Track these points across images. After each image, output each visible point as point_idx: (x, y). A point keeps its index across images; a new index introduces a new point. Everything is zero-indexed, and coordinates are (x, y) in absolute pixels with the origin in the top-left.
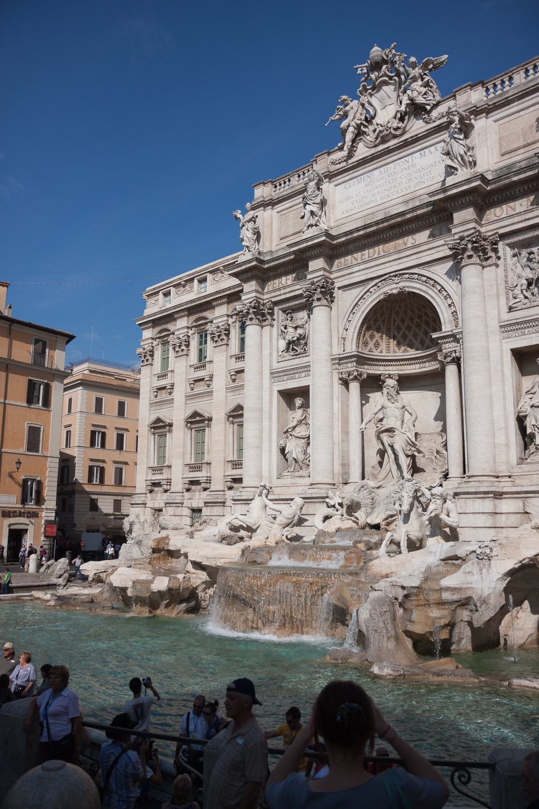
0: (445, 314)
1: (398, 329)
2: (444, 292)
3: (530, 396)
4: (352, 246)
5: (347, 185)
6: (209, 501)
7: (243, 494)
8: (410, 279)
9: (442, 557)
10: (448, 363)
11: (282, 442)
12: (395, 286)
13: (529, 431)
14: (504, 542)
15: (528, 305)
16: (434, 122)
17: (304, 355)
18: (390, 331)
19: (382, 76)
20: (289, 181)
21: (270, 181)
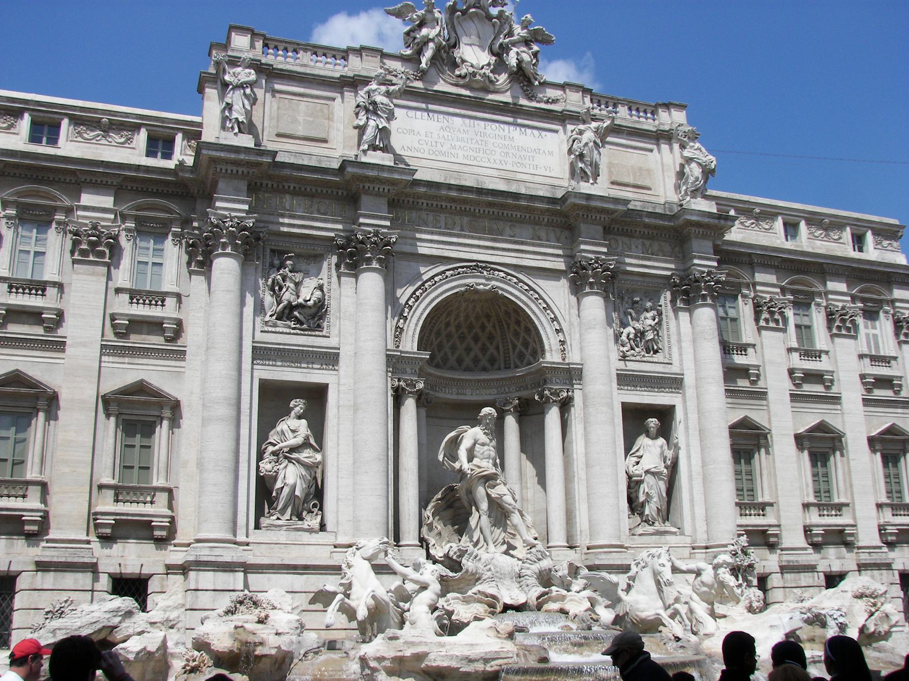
0: (550, 340)
1: (438, 334)
2: (548, 311)
3: (635, 459)
4: (425, 202)
5: (411, 113)
6: (55, 560)
7: (217, 552)
8: (502, 280)
9: (787, 631)
10: (555, 401)
11: (266, 466)
12: (483, 281)
13: (642, 498)
14: (844, 610)
15: (638, 358)
16: (538, 102)
17: (317, 333)
18: (430, 334)
19: (478, 8)
20: (295, 51)
21: (264, 36)
